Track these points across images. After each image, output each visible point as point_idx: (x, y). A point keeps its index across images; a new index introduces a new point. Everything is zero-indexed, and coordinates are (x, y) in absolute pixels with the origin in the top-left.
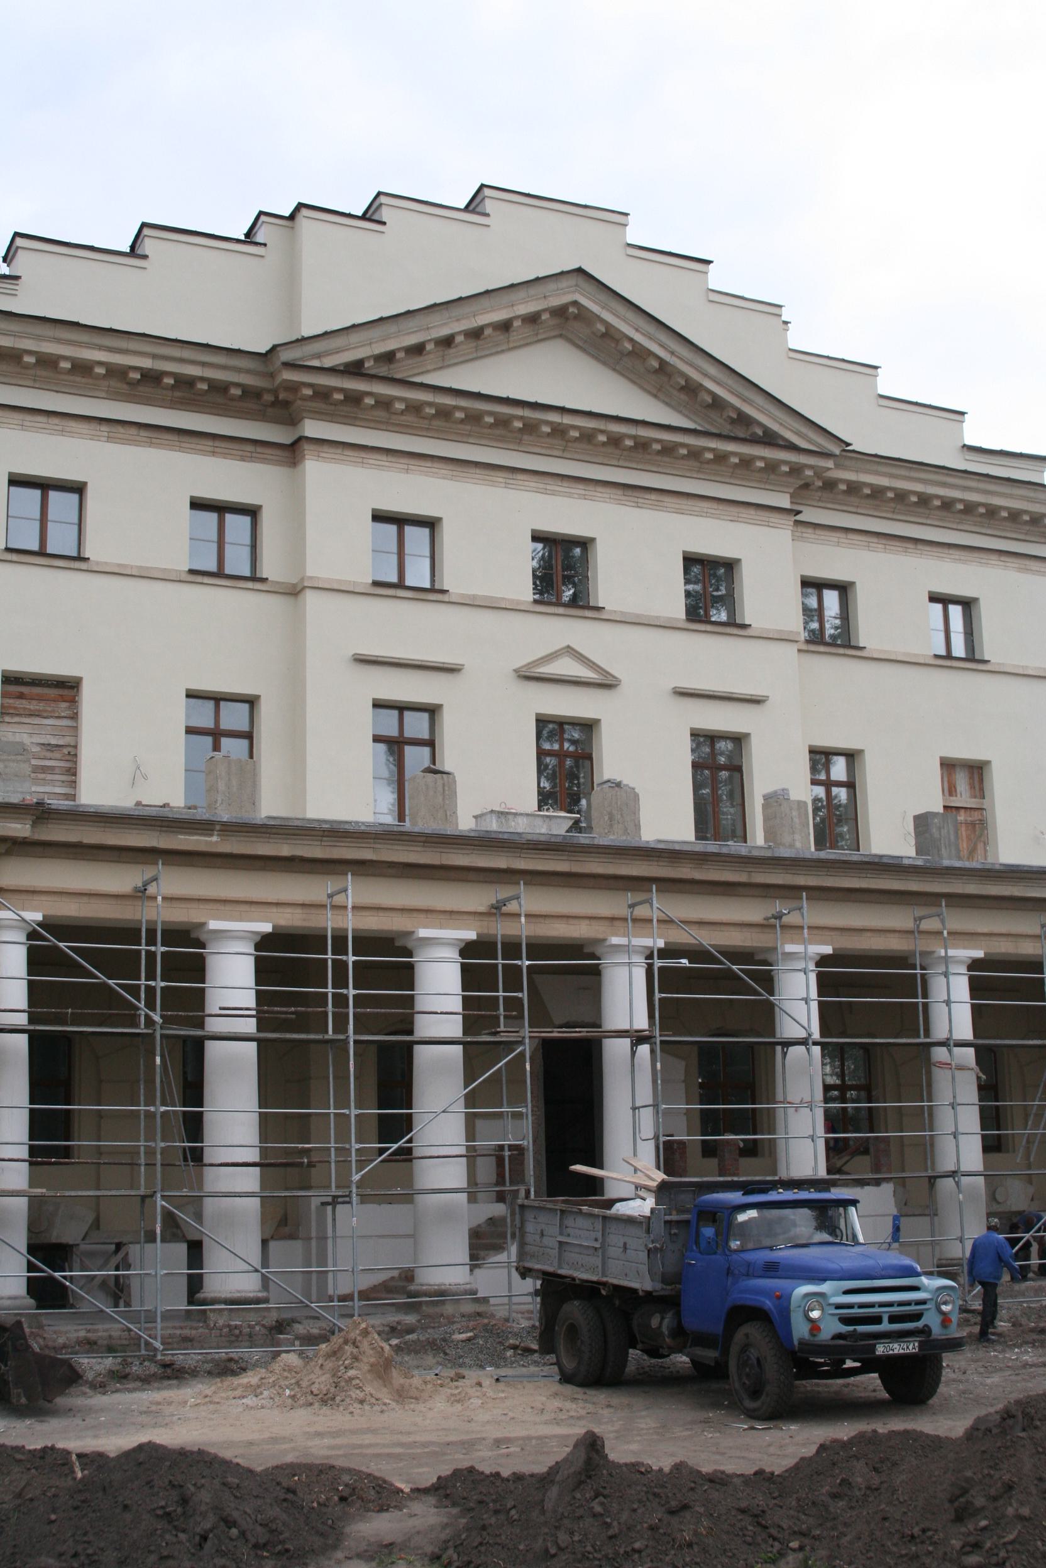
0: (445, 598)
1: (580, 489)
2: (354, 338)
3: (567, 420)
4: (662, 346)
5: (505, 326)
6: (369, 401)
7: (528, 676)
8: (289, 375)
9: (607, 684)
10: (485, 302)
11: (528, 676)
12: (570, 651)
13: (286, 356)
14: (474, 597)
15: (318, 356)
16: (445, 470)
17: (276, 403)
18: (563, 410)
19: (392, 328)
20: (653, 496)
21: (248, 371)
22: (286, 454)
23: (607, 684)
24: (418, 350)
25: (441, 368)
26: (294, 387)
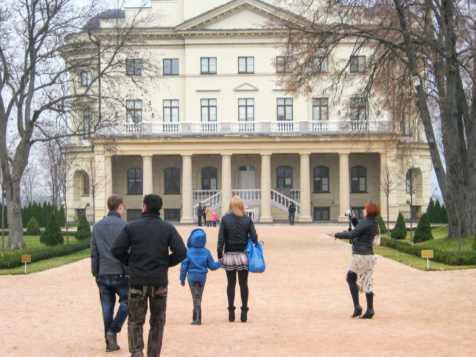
0: (217, 75)
1: (250, 46)
2: (192, 22)
3: (243, 32)
4: (268, 9)
5: (230, 11)
6: (197, 35)
7: (236, 90)
8: (178, 33)
9: (256, 90)
10: (223, 8)
11: (236, 90)
12: (246, 83)
13: (177, 29)
14: (224, 74)
15: (185, 27)
16: (217, 46)
17: (179, 37)
18: (242, 30)
19: (201, 18)
20: (269, 45)
21: (171, 32)
22: (183, 46)
23: (256, 90)
24: (209, 20)
25: (216, 22)
26: (181, 34)
